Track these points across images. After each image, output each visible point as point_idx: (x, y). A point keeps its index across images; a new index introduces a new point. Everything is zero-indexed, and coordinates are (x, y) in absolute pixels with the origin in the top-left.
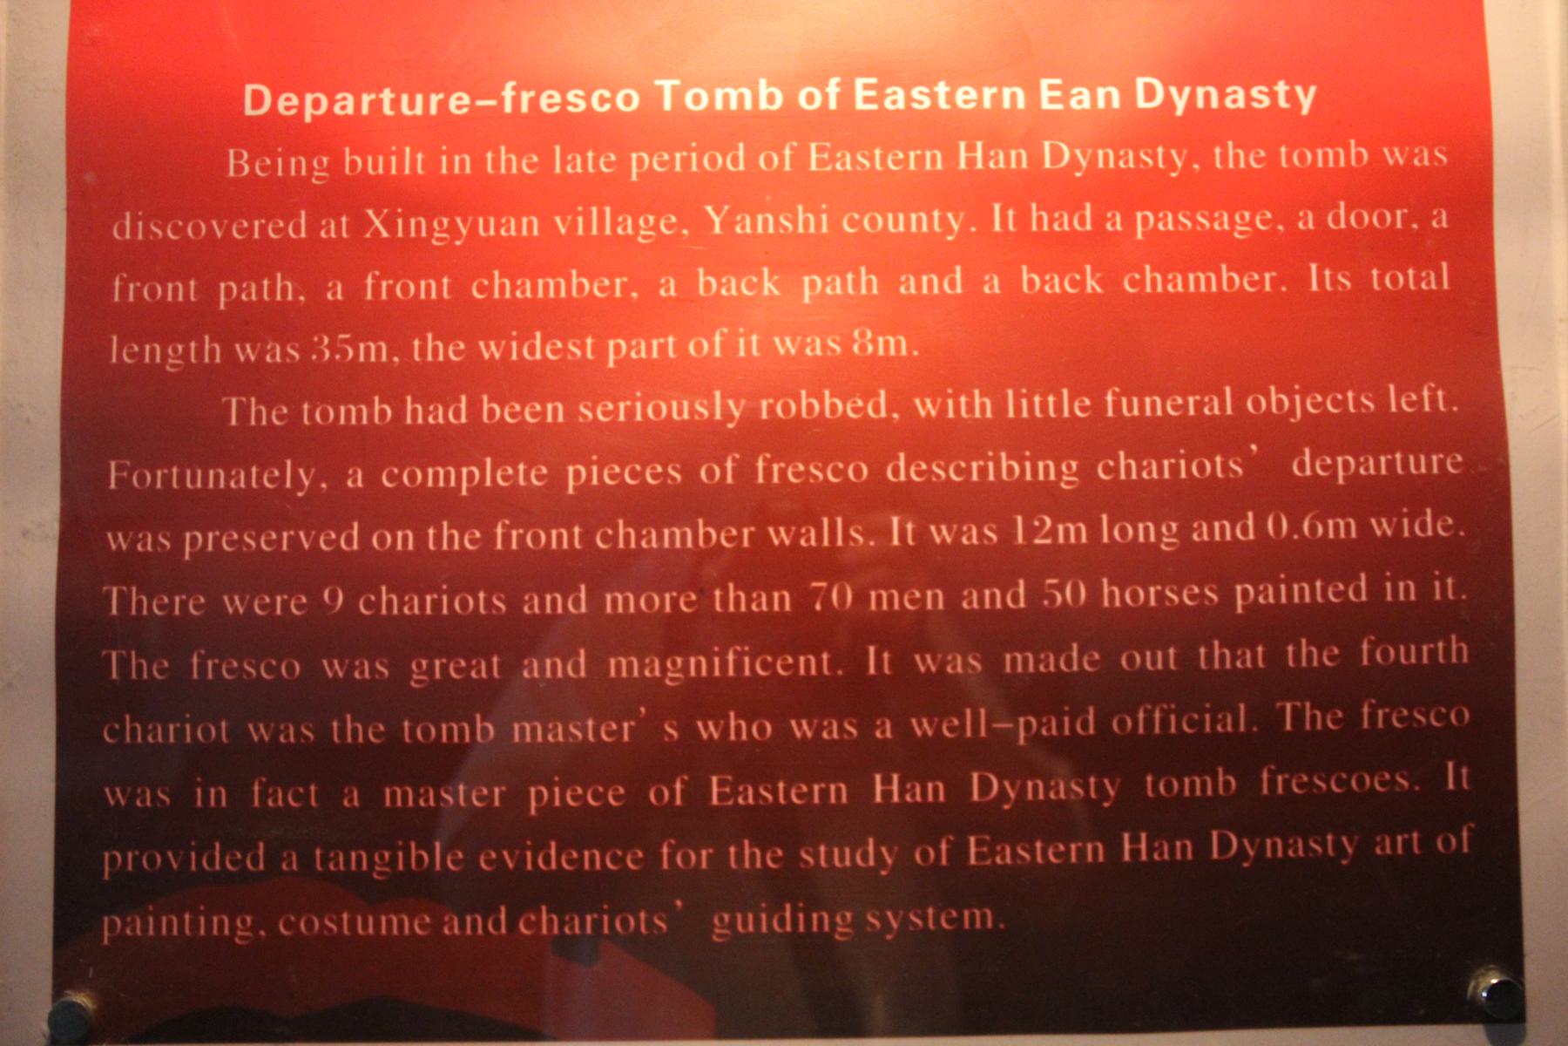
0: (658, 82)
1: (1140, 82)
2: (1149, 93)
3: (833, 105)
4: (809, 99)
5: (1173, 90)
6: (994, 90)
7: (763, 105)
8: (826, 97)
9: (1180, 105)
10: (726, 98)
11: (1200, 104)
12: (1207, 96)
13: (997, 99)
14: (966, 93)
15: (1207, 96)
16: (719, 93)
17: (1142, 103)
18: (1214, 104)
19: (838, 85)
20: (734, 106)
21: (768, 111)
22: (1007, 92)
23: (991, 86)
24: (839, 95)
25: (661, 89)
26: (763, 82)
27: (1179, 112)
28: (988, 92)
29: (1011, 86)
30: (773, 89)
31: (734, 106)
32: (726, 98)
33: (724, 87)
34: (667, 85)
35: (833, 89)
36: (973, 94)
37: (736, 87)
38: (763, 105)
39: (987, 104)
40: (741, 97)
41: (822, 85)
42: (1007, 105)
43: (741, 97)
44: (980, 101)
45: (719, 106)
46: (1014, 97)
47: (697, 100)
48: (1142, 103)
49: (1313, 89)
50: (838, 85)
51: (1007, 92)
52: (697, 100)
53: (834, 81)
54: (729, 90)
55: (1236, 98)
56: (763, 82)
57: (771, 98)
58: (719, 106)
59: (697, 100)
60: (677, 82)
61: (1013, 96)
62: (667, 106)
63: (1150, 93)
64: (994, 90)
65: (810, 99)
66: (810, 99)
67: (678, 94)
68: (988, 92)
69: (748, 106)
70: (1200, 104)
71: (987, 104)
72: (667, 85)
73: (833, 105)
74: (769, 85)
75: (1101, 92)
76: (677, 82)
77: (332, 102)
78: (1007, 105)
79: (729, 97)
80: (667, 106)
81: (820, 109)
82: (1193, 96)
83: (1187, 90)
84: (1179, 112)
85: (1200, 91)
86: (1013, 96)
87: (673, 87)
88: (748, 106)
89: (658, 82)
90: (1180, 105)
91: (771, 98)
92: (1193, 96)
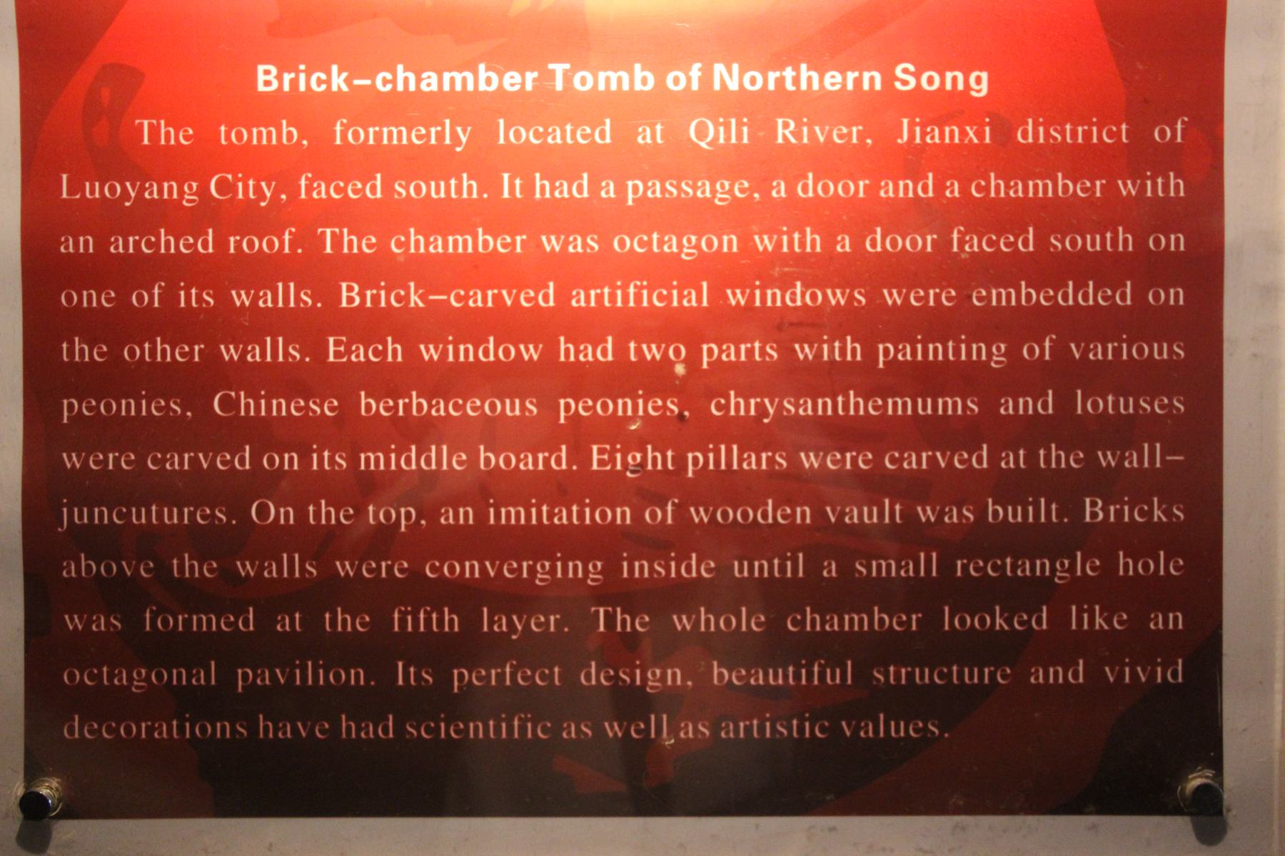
0: (551, 66)
3: (695, 86)
4: (676, 81)
6: (856, 74)
8: (689, 80)
10: (608, 80)
13: (858, 82)
19: (700, 70)
20: (614, 87)
22: (866, 75)
24: (700, 79)
25: (553, 72)
26: (638, 67)
28: (851, 76)
31: (614, 87)
34: (559, 68)
35: (696, 71)
36: (839, 78)
37: (616, 71)
39: (850, 86)
40: (620, 80)
42: (866, 86)
43: (620, 80)
45: (602, 87)
46: (872, 79)
50: (700, 70)
51: (866, 75)
54: (610, 73)
56: (638, 67)
57: (644, 81)
58: (602, 87)
59: (584, 82)
61: (872, 79)
62: (559, 86)
64: (856, 74)
65: (676, 81)
66: (676, 81)
67: (568, 78)
68: (851, 76)
69: (626, 87)
74: (643, 69)
75: (949, 75)
76: (567, 66)
77: (419, 80)
78: (866, 86)
79: (610, 79)
80: (559, 86)
81: (684, 90)
86: (872, 79)
87: (565, 73)
88: (626, 87)
89: (551, 66)
91: (644, 81)
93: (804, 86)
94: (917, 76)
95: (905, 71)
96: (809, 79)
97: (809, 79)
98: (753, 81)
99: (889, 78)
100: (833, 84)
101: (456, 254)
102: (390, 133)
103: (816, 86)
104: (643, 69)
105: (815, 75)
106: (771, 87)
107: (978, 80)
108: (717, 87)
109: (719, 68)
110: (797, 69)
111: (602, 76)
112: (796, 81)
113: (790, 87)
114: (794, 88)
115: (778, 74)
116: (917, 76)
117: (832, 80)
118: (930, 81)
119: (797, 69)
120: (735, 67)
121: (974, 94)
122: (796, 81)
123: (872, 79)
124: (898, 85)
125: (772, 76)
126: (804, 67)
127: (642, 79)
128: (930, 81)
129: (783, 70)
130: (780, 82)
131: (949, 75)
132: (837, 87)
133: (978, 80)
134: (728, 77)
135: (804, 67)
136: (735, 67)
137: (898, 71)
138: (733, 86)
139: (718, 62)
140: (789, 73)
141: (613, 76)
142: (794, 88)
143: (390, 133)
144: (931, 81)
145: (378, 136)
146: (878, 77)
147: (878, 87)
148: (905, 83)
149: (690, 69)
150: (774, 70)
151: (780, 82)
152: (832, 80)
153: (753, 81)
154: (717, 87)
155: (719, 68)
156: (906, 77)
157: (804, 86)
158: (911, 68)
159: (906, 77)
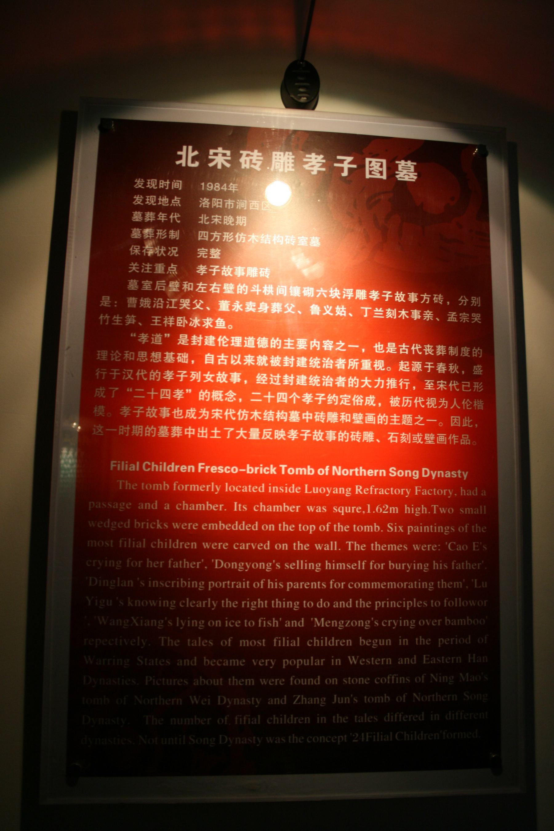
0: (281, 466)
1: (424, 469)
2: (426, 473)
3: (327, 474)
5: (432, 472)
7: (309, 473)
8: (325, 471)
9: (434, 476)
10: (299, 471)
11: (439, 476)
12: (441, 474)
13: (378, 473)
15: (441, 474)
16: (297, 469)
17: (424, 476)
18: (443, 476)
20: (301, 473)
21: (310, 475)
22: (381, 471)
26: (309, 467)
27: (433, 478)
28: (376, 471)
29: (382, 469)
30: (312, 469)
31: (301, 473)
32: (299, 471)
33: (298, 467)
34: (283, 466)
37: (302, 467)
39: (375, 475)
40: (303, 471)
41: (324, 468)
42: (381, 475)
43: (303, 471)
44: (374, 474)
45: (297, 473)
46: (382, 472)
47: (291, 471)
48: (424, 476)
49: (467, 473)
52: (291, 471)
53: (327, 467)
55: (448, 474)
56: (309, 467)
57: (311, 472)
59: (291, 471)
60: (286, 466)
61: (383, 473)
62: (283, 473)
63: (426, 472)
65: (321, 472)
66: (321, 472)
67: (286, 469)
70: (439, 476)
72: (283, 466)
74: (311, 467)
76: (286, 466)
79: (300, 471)
80: (283, 473)
82: (437, 473)
83: (436, 472)
84: (433, 478)
85: (439, 472)
86: (383, 473)
88: (305, 473)
89: (281, 466)
90: (434, 476)
91: (311, 472)
92: (437, 473)
93: (361, 475)
94: (396, 471)
95: (393, 470)
96: (363, 472)
97: (363, 472)
98: (345, 472)
99: (388, 472)
103: (365, 475)
104: (311, 467)
105: (365, 471)
106: (351, 474)
107: (416, 473)
108: (334, 474)
109: (334, 468)
111: (297, 469)
112: (359, 472)
113: (357, 474)
115: (353, 470)
116: (396, 471)
117: (370, 473)
118: (401, 473)
119: (359, 468)
120: (340, 467)
121: (414, 478)
122: (359, 472)
123: (382, 472)
124: (390, 475)
125: (351, 471)
126: (361, 468)
127: (309, 471)
128: (401, 473)
129: (354, 468)
130: (354, 472)
131: (406, 472)
132: (372, 475)
133: (416, 473)
134: (338, 471)
135: (361, 468)
136: (340, 467)
137: (391, 470)
138: (339, 474)
139: (334, 465)
140: (356, 470)
141: (301, 470)
144: (401, 473)
145: (189, 488)
146: (384, 471)
147: (385, 475)
148: (393, 474)
150: (352, 469)
151: (354, 472)
152: (370, 473)
153: (345, 472)
154: (334, 474)
155: (334, 468)
156: (393, 472)
158: (395, 469)
159: (393, 472)
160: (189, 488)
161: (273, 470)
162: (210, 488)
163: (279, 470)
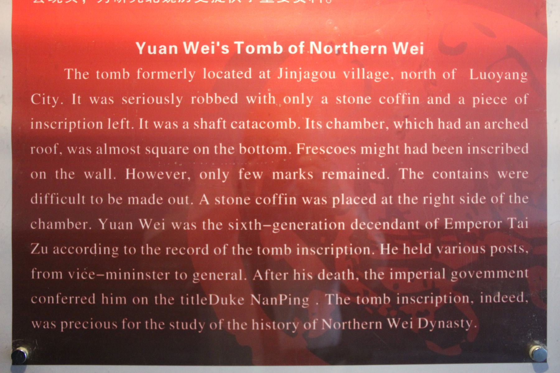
0: (235, 43)
3: (301, 52)
4: (292, 49)
6: (375, 47)
7: (275, 52)
8: (299, 49)
10: (261, 49)
13: (376, 50)
14: (365, 48)
19: (303, 44)
20: (264, 52)
21: (277, 54)
22: (380, 47)
23: (374, 45)
24: (304, 48)
25: (236, 45)
26: (275, 43)
28: (373, 47)
31: (264, 52)
32: (261, 49)
34: (239, 43)
35: (301, 46)
36: (367, 49)
38: (275, 52)
39: (372, 52)
40: (267, 49)
41: (298, 45)
42: (380, 52)
43: (267, 49)
44: (370, 51)
45: (259, 52)
47: (250, 49)
50: (303, 44)
51: (380, 47)
52: (250, 49)
53: (302, 43)
54: (262, 46)
56: (275, 43)
57: (278, 49)
58: (259, 52)
59: (250, 50)
60: (243, 43)
61: (382, 49)
62: (239, 52)
64: (375, 47)
65: (293, 49)
66: (293, 49)
67: (243, 48)
68: (373, 47)
71: (372, 52)
72: (239, 43)
73: (301, 52)
74: (277, 44)
76: (243, 43)
78: (380, 52)
79: (263, 49)
80: (239, 52)
86: (382, 49)
87: (241, 45)
88: (270, 52)
89: (235, 43)
91: (278, 49)
93: (351, 52)
96: (354, 49)
97: (354, 49)
100: (365, 51)
101: (354, 130)
102: (161, 74)
103: (357, 52)
105: (356, 47)
108: (311, 52)
109: (312, 44)
110: (348, 44)
112: (348, 49)
113: (345, 52)
114: (347, 53)
115: (339, 46)
117: (364, 49)
119: (348, 44)
120: (320, 43)
122: (348, 49)
126: (351, 43)
127: (277, 49)
129: (341, 44)
132: (367, 53)
135: (351, 43)
136: (320, 43)
138: (319, 52)
140: (344, 46)
141: (264, 47)
142: (347, 53)
143: (161, 74)
145: (156, 75)
146: (385, 48)
149: (299, 44)
153: (328, 49)
157: (351, 52)
160: (156, 75)
161: (225, 49)
162: (182, 75)
163: (233, 48)
